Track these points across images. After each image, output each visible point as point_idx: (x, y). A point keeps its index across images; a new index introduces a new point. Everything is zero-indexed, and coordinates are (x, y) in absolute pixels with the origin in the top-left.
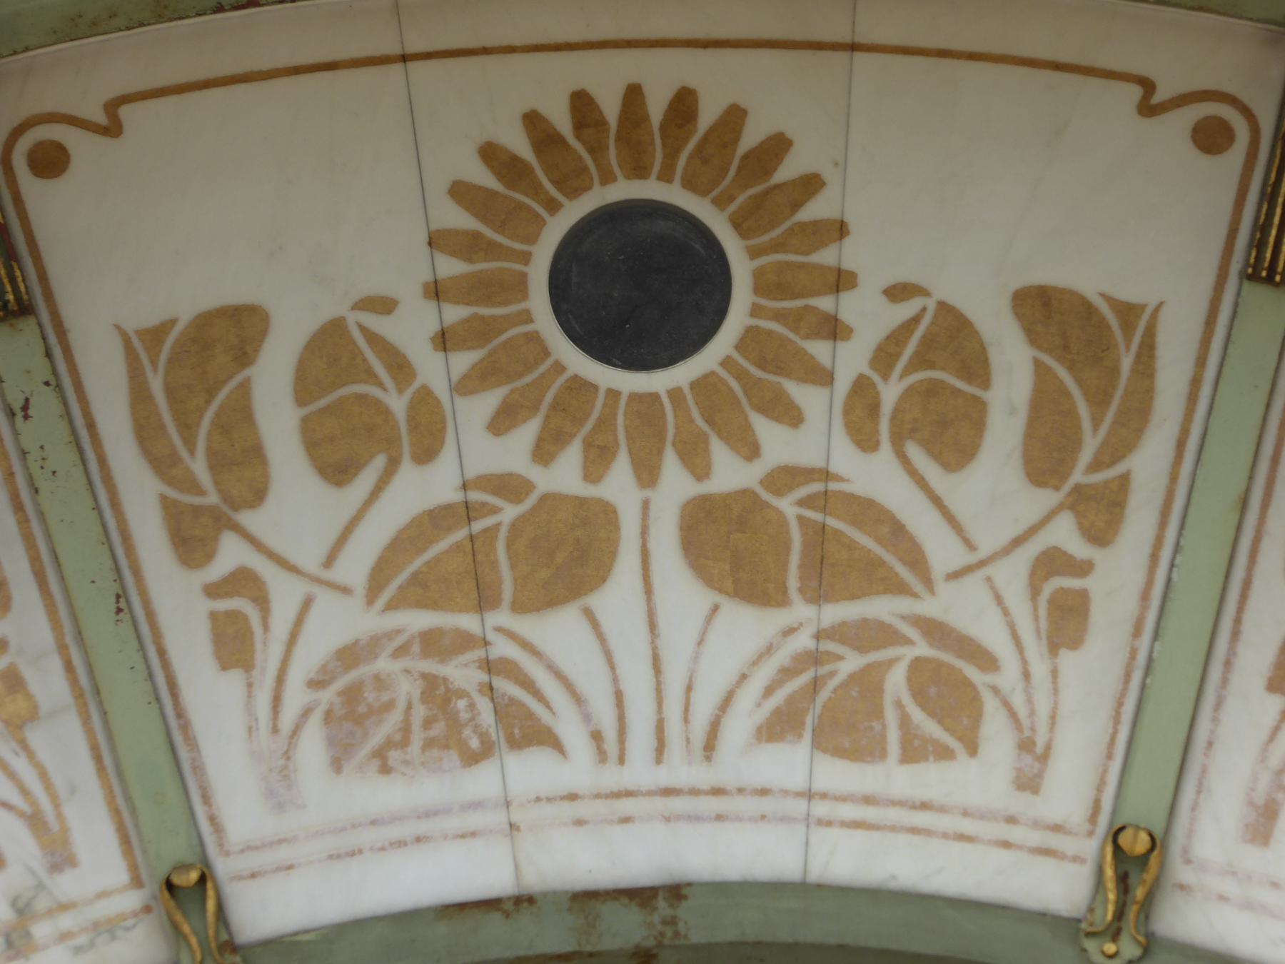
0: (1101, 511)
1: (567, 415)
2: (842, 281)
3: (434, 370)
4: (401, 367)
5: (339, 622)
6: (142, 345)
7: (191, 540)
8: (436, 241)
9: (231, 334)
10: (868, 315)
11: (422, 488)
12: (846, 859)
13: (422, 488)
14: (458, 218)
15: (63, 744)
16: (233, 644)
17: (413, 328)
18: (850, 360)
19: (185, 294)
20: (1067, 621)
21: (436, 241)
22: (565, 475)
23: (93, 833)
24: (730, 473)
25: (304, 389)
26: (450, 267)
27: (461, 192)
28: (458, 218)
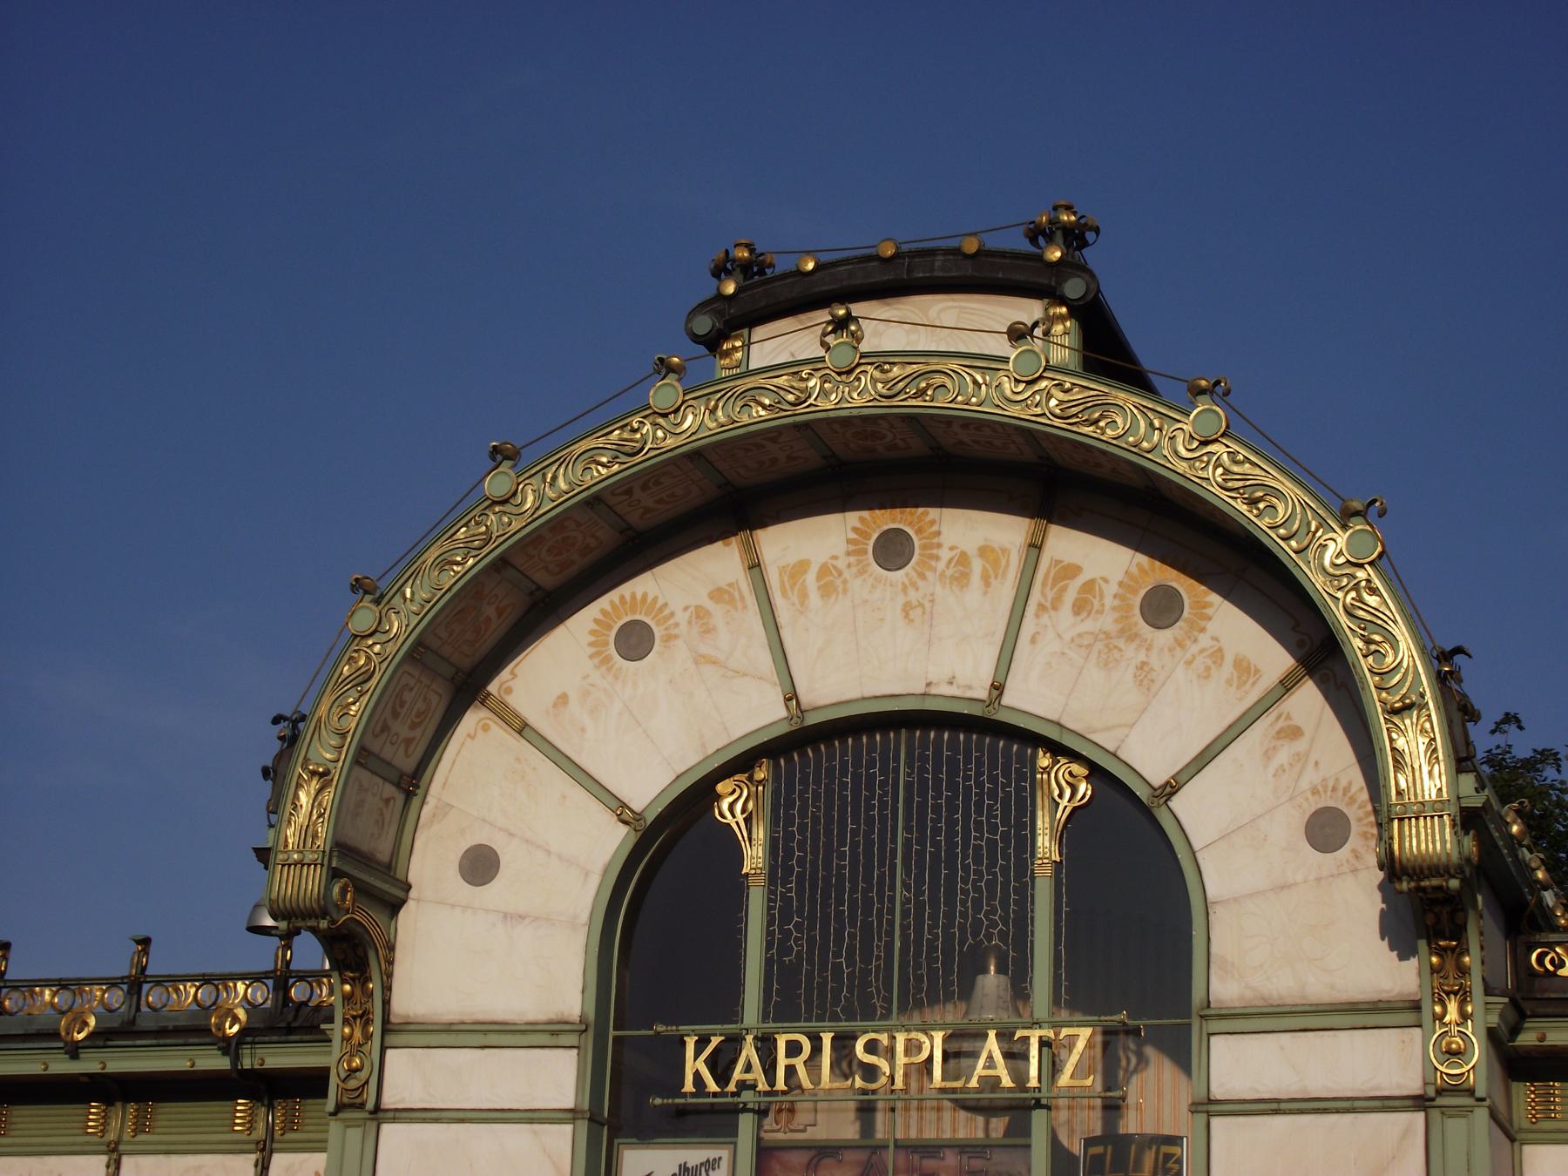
2: (939, 546)
3: (847, 574)
4: (840, 574)
6: (782, 570)
8: (848, 541)
9: (803, 566)
10: (945, 554)
14: (853, 536)
18: (941, 565)
19: (792, 559)
21: (848, 541)
25: (819, 578)
26: (851, 548)
27: (855, 530)
28: (853, 536)
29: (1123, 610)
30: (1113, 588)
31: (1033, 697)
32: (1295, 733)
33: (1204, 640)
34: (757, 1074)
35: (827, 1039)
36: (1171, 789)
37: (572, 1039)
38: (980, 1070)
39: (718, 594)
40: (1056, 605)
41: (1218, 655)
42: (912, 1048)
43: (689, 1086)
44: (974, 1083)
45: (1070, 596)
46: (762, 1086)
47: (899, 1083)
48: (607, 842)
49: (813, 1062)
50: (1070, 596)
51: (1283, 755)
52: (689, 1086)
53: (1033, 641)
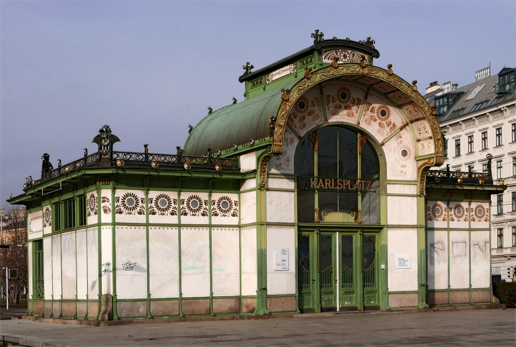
0: (358, 108)
1: (341, 101)
5: (332, 109)
7: (327, 105)
9: (329, 96)
10: (351, 98)
11: (335, 104)
12: (349, 121)
13: (335, 104)
15: (322, 113)
16: (328, 110)
17: (336, 96)
18: (351, 100)
19: (328, 94)
20: (357, 112)
22: (340, 104)
23: (323, 117)
24: (346, 104)
29: (378, 112)
30: (376, 109)
31: (363, 126)
32: (401, 137)
33: (389, 120)
34: (322, 185)
35: (333, 180)
36: (383, 144)
37: (294, 177)
38: (355, 187)
39: (316, 99)
40: (368, 110)
41: (391, 123)
42: (346, 182)
43: (312, 187)
44: (355, 189)
45: (370, 109)
46: (323, 187)
47: (344, 188)
48: (296, 142)
49: (331, 184)
50: (370, 109)
51: (399, 141)
52: (312, 187)
53: (364, 115)
